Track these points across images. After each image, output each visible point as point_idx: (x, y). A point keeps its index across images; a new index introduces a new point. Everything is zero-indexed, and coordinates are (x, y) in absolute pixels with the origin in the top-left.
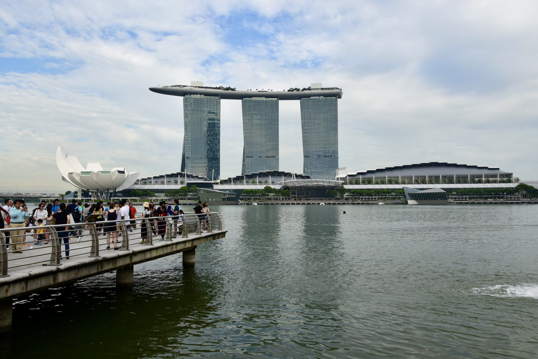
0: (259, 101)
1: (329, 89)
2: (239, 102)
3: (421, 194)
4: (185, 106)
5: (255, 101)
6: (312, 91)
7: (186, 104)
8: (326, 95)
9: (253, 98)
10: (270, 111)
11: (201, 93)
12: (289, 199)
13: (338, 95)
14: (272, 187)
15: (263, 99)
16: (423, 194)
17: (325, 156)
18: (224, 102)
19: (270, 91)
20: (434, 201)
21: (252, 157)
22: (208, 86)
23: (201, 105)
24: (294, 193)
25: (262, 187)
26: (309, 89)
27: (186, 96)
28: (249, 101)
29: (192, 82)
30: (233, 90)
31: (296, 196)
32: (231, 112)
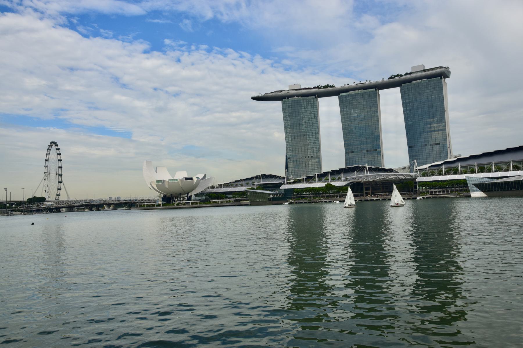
0: (355, 95)
1: (431, 69)
2: (336, 99)
3: (495, 183)
4: (284, 109)
5: (352, 95)
6: (413, 75)
7: (284, 107)
8: (428, 77)
9: (351, 92)
10: (369, 102)
11: (298, 95)
12: (362, 195)
13: (442, 74)
14: (333, 183)
15: (361, 91)
16: (499, 183)
17: (432, 145)
18: (322, 102)
19: (368, 82)
20: (495, 193)
21: (352, 152)
22: (307, 87)
23: (298, 106)
24: (367, 189)
25: (323, 185)
26: (411, 73)
27: (341, 94)
28: (346, 96)
29: (289, 86)
30: (332, 86)
31: (370, 191)
32: (329, 109)
